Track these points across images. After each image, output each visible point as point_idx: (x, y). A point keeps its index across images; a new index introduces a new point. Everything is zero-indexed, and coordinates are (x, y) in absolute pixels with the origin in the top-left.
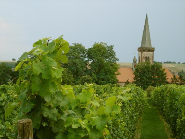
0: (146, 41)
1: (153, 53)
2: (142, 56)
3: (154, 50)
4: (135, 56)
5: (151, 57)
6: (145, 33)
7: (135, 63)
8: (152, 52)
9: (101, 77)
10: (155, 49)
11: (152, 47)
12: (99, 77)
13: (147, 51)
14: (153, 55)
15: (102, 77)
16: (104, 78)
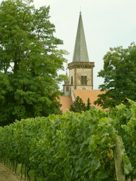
0: (81, 52)
1: (92, 69)
2: (75, 75)
3: (94, 66)
4: (67, 73)
5: (89, 77)
6: (80, 41)
7: (67, 84)
8: (91, 69)
9: (21, 81)
10: (95, 64)
11: (91, 60)
12: (16, 82)
13: (83, 68)
14: (92, 74)
15: (25, 81)
16: (30, 85)
